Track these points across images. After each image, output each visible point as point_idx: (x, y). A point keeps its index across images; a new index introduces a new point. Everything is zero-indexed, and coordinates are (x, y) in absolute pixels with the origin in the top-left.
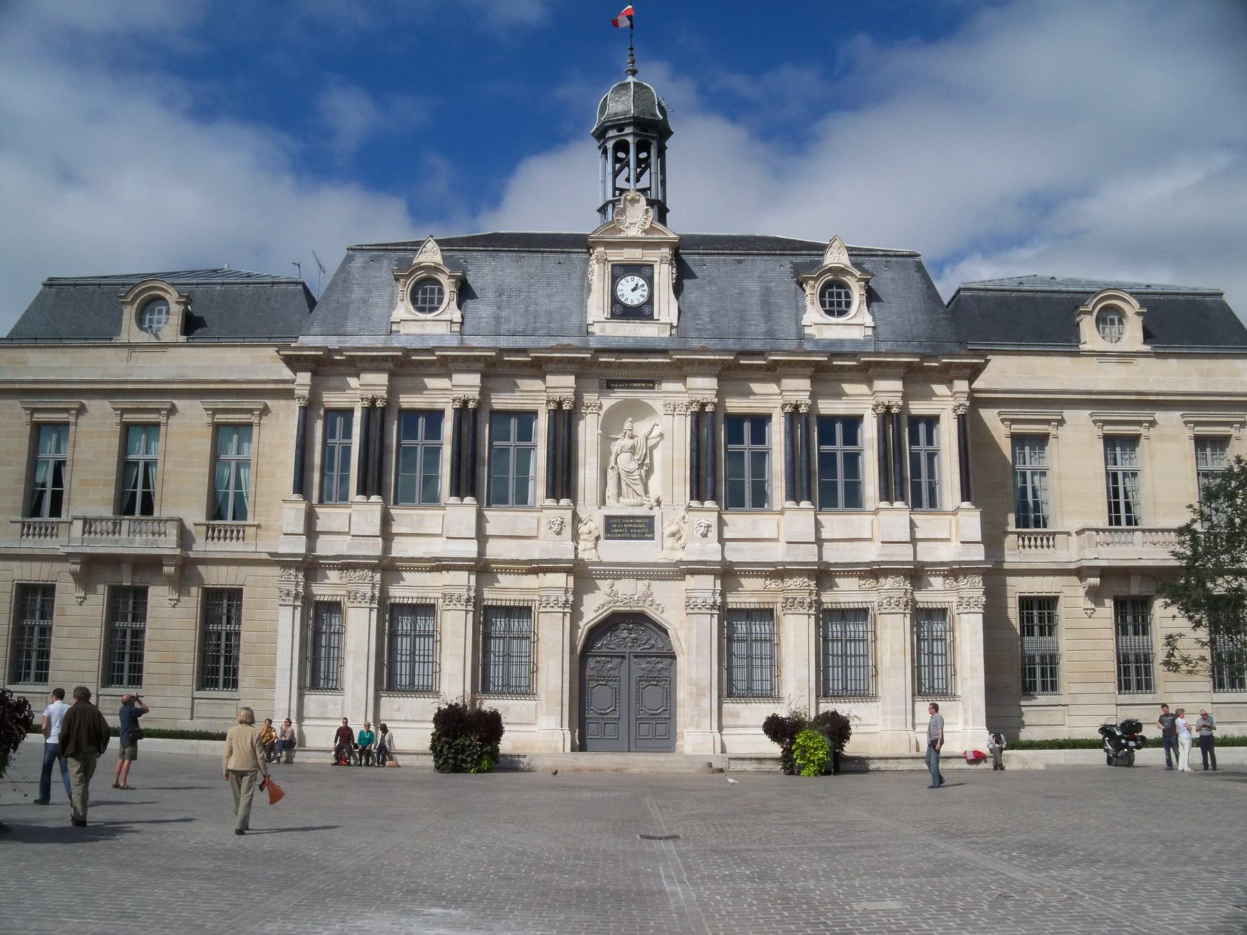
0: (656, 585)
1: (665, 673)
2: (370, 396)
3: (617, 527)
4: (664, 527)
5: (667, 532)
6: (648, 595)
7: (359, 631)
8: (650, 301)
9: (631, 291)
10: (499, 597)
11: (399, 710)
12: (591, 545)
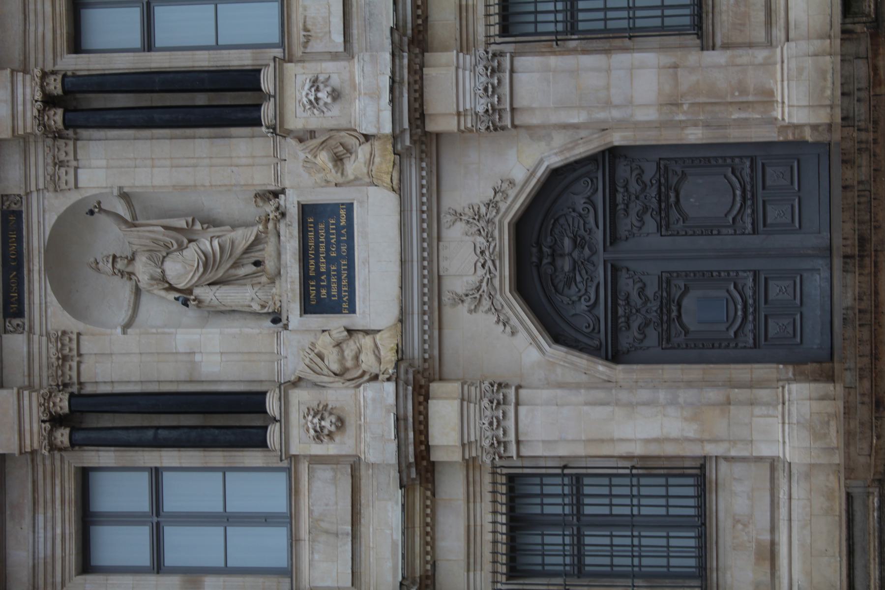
3: (326, 288)
5: (334, 176)
10: (488, 548)
12: (367, 341)
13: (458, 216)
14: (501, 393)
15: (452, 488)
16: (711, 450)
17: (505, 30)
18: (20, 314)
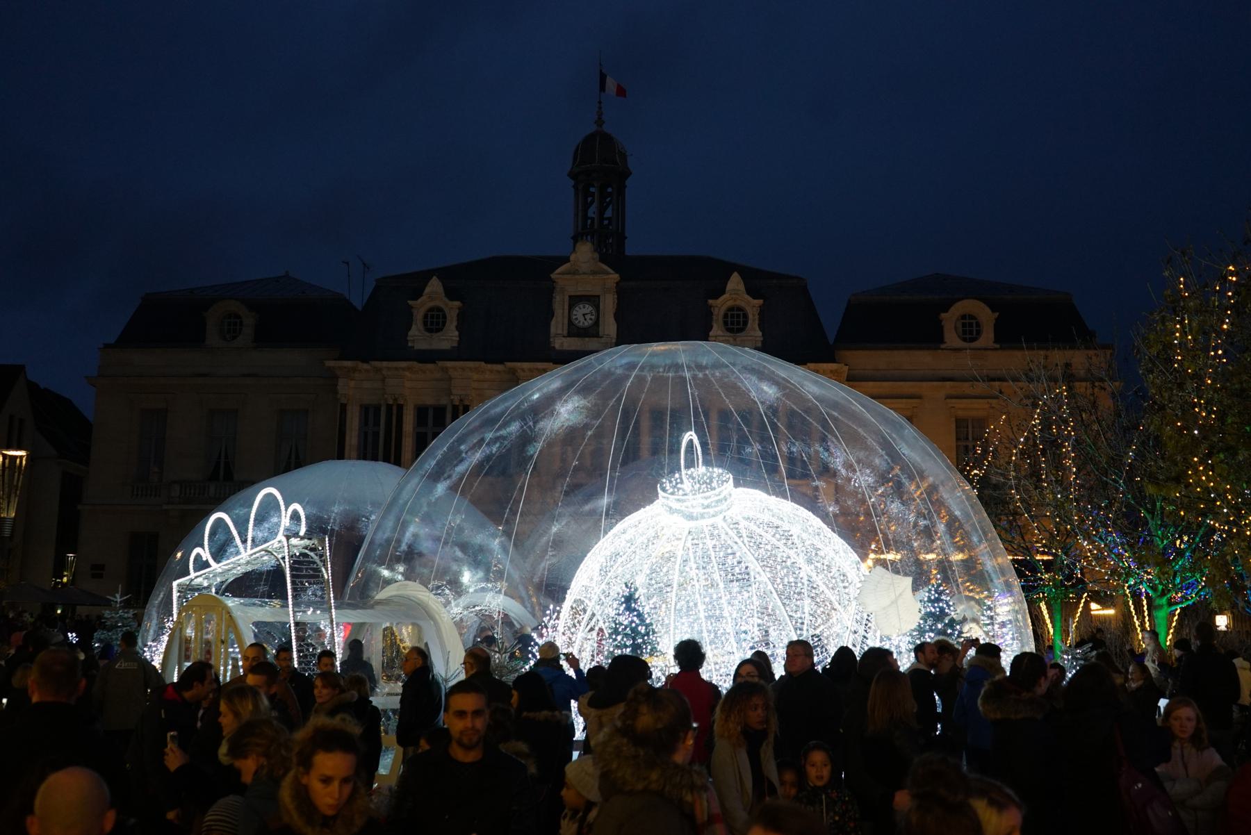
8: (597, 323)
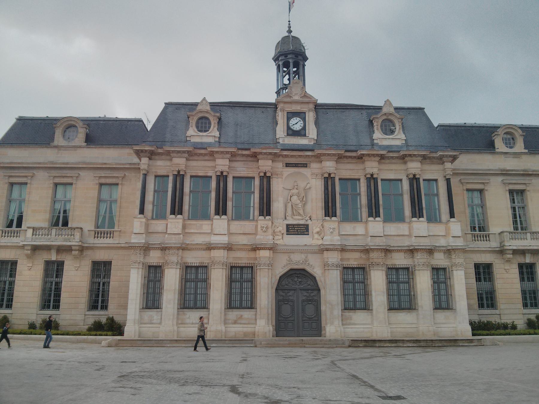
0: (310, 256)
1: (315, 298)
2: (177, 169)
3: (292, 229)
4: (314, 228)
5: (314, 232)
6: (306, 261)
7: (172, 279)
8: (304, 128)
9: (296, 124)
10: (238, 262)
11: (189, 318)
12: (280, 237)
13: (306, 257)
14: (271, 265)
15: (252, 255)
16: (258, 310)
17: (344, 268)
18: (286, 166)
